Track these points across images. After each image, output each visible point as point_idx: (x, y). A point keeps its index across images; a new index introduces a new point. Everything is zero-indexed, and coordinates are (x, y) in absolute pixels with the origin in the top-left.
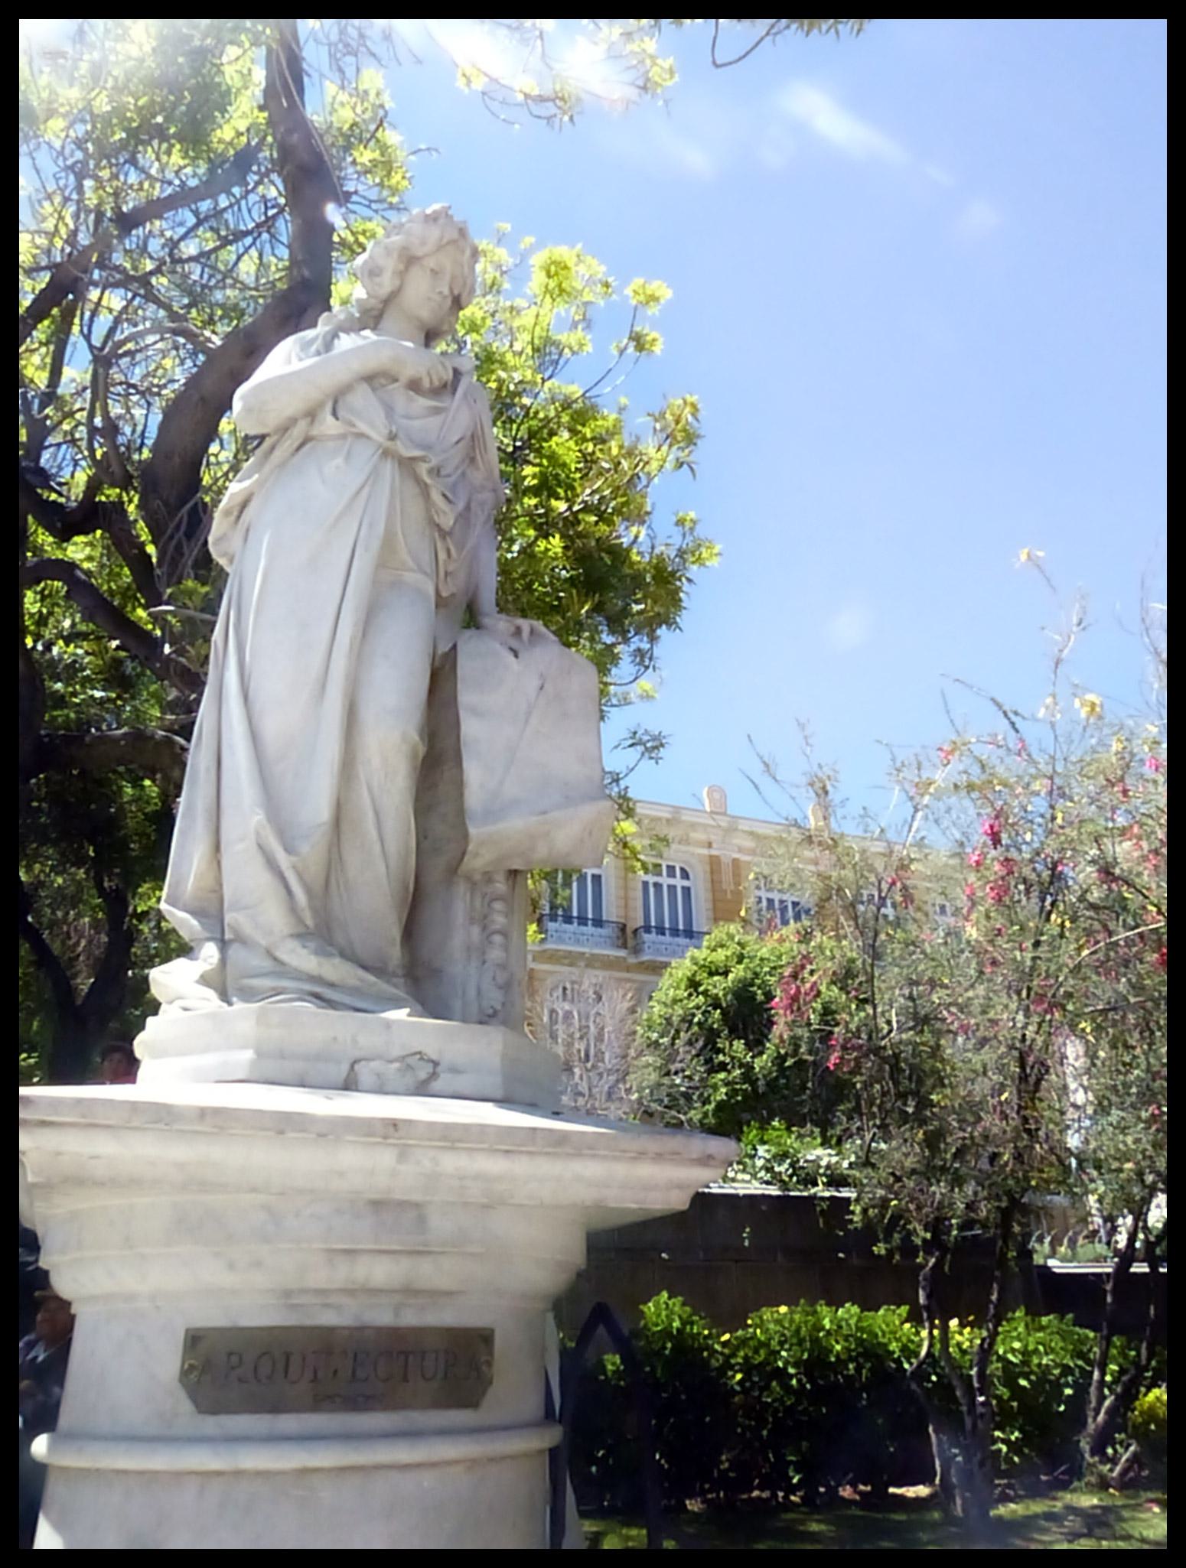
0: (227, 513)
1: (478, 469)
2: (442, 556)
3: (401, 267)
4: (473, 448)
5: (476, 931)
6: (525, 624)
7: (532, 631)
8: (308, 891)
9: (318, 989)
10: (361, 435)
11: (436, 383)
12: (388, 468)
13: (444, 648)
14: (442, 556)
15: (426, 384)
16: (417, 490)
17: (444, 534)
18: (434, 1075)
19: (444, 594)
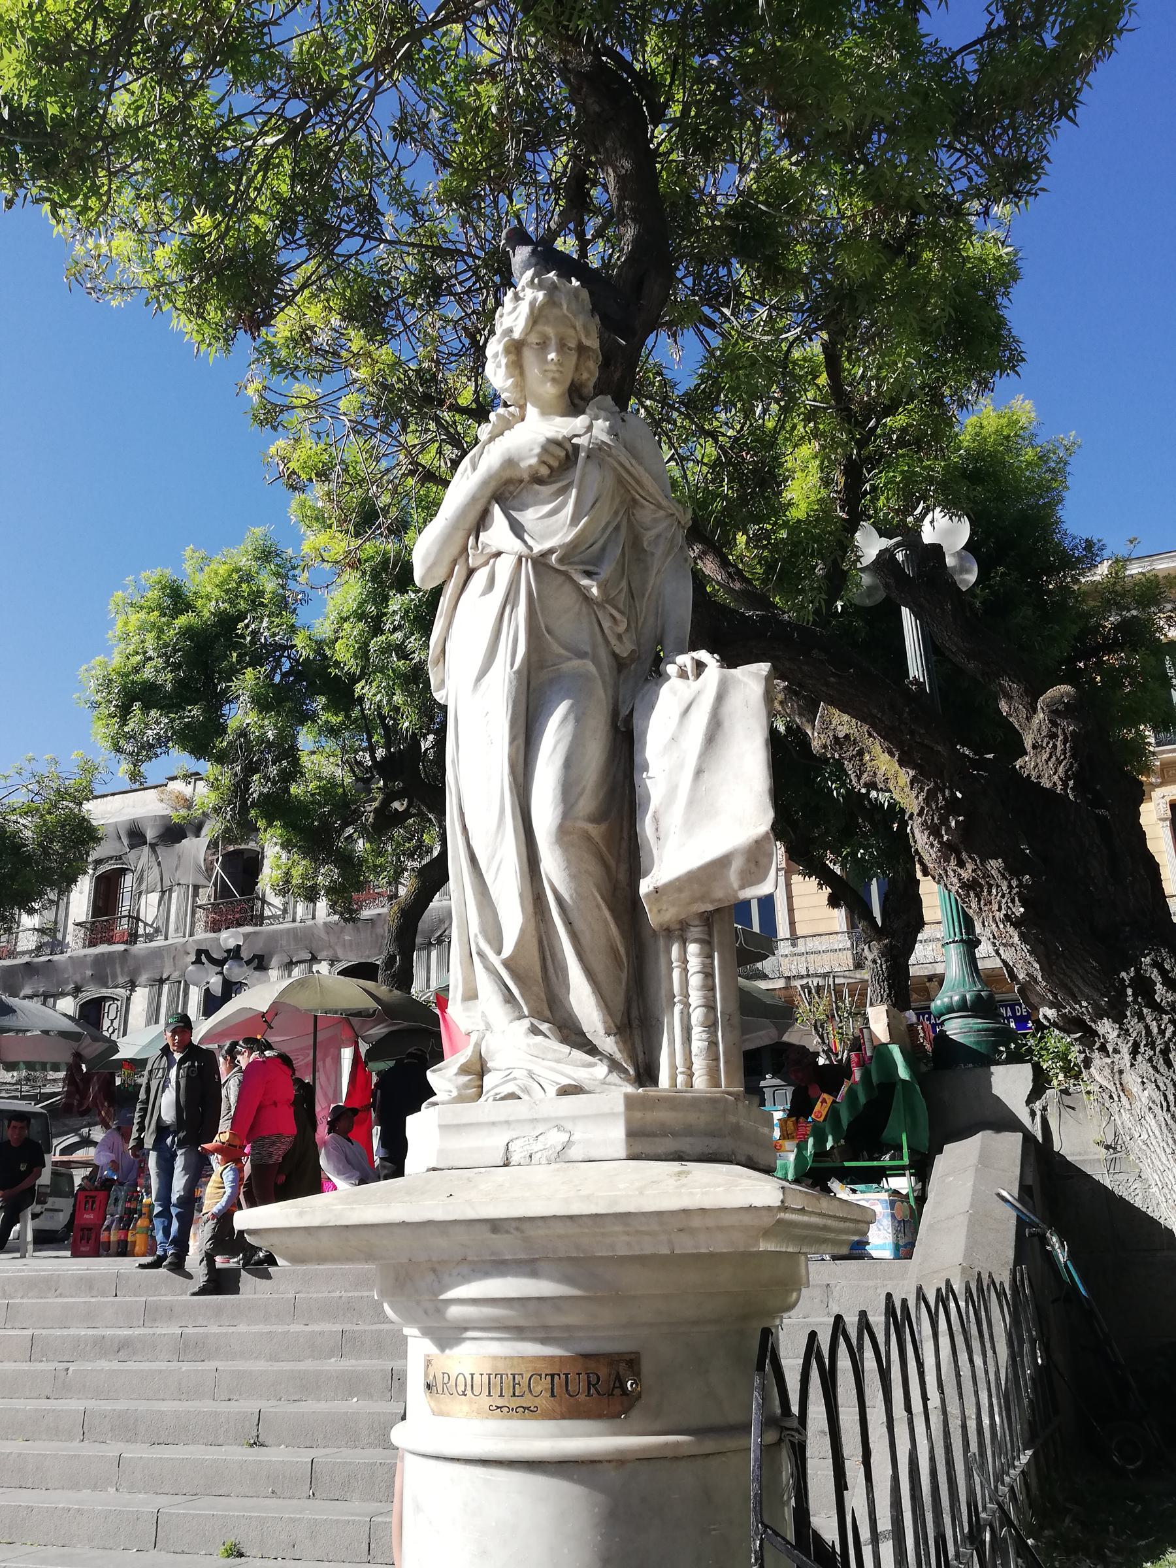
1: (643, 507)
2: (606, 625)
3: (513, 357)
10: (498, 554)
11: (555, 464)
13: (624, 712)
15: (544, 471)
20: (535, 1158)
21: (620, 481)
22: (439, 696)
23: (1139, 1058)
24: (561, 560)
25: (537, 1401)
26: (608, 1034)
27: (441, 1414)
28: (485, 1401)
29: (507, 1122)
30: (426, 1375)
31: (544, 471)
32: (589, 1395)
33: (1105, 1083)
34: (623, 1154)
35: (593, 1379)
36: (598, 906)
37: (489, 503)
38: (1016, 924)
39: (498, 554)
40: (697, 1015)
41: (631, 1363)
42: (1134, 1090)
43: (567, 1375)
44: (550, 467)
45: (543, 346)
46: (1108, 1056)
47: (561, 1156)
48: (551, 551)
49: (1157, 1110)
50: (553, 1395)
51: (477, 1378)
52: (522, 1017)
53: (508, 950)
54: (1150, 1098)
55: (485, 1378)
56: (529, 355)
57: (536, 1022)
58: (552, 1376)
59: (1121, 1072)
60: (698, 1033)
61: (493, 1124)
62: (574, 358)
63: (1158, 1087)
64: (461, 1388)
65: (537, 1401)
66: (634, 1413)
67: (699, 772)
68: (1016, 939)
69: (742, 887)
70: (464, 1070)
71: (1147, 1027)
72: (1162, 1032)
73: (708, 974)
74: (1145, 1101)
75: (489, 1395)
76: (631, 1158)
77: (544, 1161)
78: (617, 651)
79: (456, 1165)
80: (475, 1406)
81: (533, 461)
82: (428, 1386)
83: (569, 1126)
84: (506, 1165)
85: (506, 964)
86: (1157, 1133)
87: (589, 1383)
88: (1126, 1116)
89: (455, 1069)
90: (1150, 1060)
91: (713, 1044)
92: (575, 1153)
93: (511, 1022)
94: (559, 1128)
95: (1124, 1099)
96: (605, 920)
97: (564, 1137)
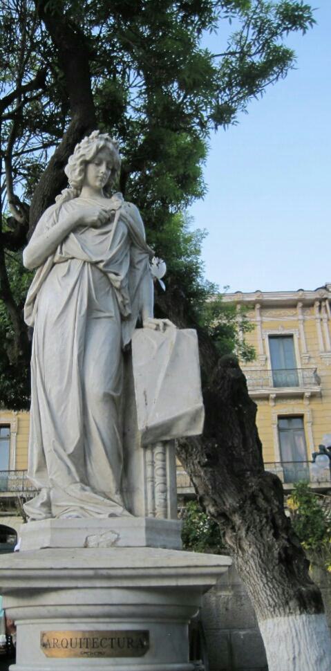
0: (29, 304)
2: (120, 299)
4: (131, 239)
5: (149, 469)
6: (160, 321)
7: (165, 324)
8: (74, 463)
9: (82, 506)
10: (73, 258)
11: (104, 221)
12: (88, 268)
13: (126, 342)
14: (120, 299)
15: (99, 224)
16: (102, 275)
17: (119, 290)
18: (118, 539)
19: (126, 315)
20: (100, 545)
21: (129, 233)
22: (28, 322)
23: (250, 533)
24: (105, 266)
25: (104, 650)
26: (116, 493)
27: (52, 656)
28: (78, 650)
29: (86, 528)
30: (42, 640)
31: (99, 224)
32: (128, 647)
33: (232, 545)
34: (144, 544)
35: (130, 641)
36: (115, 433)
37: (69, 234)
38: (204, 466)
39: (73, 258)
40: (159, 487)
41: (145, 634)
42: (246, 547)
43: (119, 639)
44: (101, 222)
45: (99, 164)
46: (235, 531)
47: (113, 544)
48: (102, 261)
49: (256, 557)
50: (112, 647)
51: (74, 641)
52: (76, 482)
53: (71, 449)
54: (253, 552)
55: (78, 641)
56: (91, 168)
57: (83, 485)
58: (112, 639)
59: (240, 539)
60: (158, 495)
61: (79, 529)
62: (110, 173)
63: (257, 547)
64: (65, 645)
65: (104, 650)
66: (147, 655)
67: (167, 376)
68: (202, 474)
69: (186, 430)
70: (43, 504)
71: (254, 519)
72: (261, 521)
73: (164, 469)
74: (250, 552)
75: (81, 647)
76: (147, 546)
77: (105, 546)
78: (123, 313)
79: (60, 546)
80: (72, 653)
81: (96, 218)
82: (44, 645)
83: (118, 531)
84: (86, 547)
85: (69, 456)
86: (254, 567)
87: (128, 642)
88: (240, 560)
89: (39, 504)
90: (254, 534)
91: (165, 500)
92: (120, 543)
93: (71, 484)
94: (113, 532)
95: (240, 552)
96: (117, 440)
97: (116, 536)
